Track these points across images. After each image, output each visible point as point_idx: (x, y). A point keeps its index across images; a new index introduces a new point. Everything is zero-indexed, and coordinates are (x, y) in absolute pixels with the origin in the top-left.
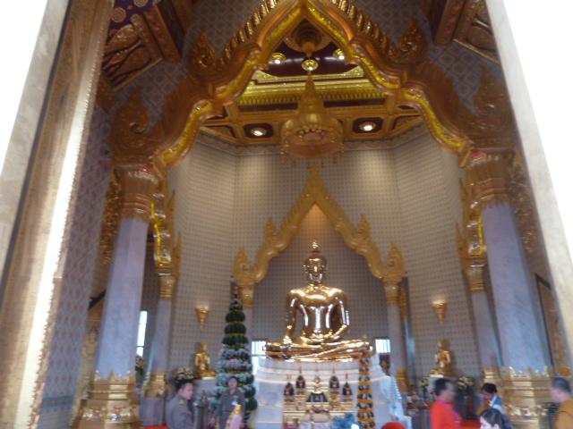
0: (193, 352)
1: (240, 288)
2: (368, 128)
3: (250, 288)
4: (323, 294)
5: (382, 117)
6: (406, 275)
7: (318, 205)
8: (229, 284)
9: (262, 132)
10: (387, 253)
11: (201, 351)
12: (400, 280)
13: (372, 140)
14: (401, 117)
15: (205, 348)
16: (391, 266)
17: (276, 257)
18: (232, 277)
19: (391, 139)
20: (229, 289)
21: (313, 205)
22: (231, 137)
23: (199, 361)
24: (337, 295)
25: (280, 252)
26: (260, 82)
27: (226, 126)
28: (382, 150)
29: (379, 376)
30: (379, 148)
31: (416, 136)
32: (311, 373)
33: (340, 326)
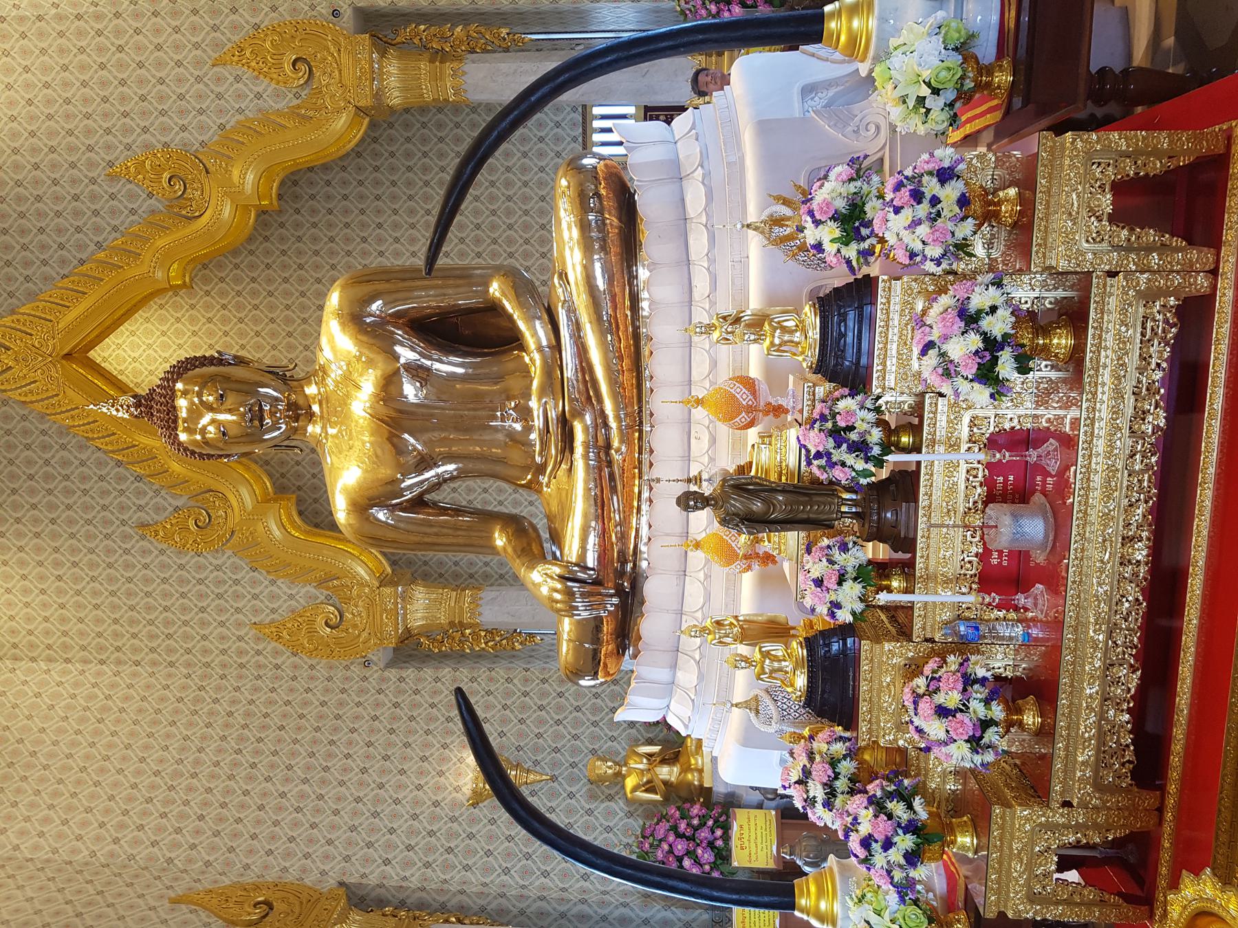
0: (619, 806)
3: (406, 598)
4: (348, 380)
6: (347, 13)
8: (392, 674)
10: (262, 85)
11: (619, 777)
15: (606, 768)
17: (299, 501)
18: (367, 664)
20: (410, 673)
23: (650, 787)
24: (355, 319)
25: (281, 490)
29: (730, 125)
32: (700, 446)
33: (494, 308)
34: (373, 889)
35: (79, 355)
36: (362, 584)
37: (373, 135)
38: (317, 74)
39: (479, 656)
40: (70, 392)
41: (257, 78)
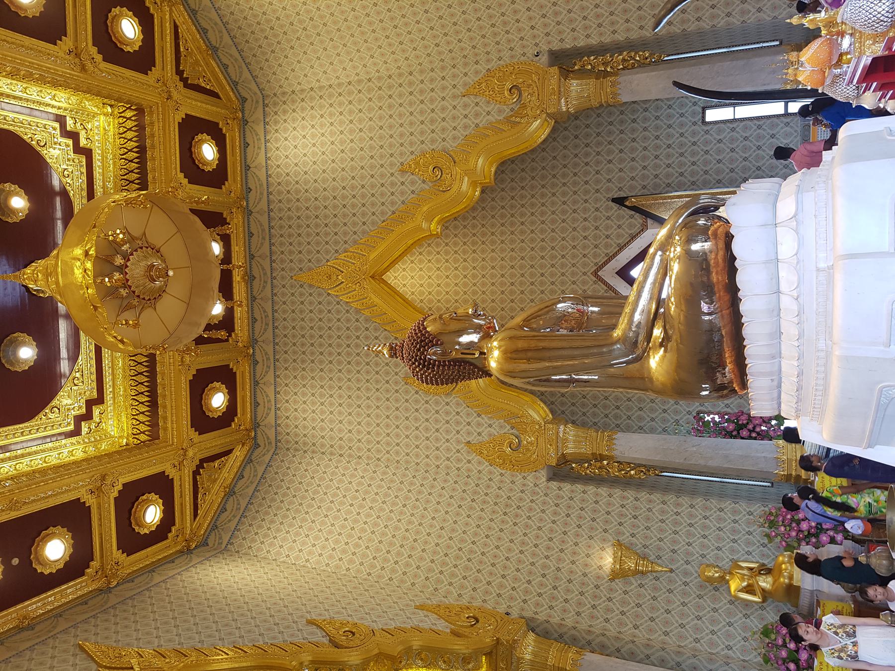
1: (564, 460)
2: (208, 152)
5: (179, 117)
7: (387, 269)
9: (218, 390)
12: (555, 70)
13: (247, 145)
14: (179, 73)
16: (520, 95)
19: (244, 100)
21: (385, 282)
22: (232, 457)
26: (95, 395)
27: (196, 473)
28: (266, 123)
30: (260, 129)
31: (227, 39)
34: (541, 623)
35: (378, 277)
36: (534, 422)
37: (553, 136)
38: (525, 94)
39: (614, 482)
40: (373, 296)
41: (488, 102)
